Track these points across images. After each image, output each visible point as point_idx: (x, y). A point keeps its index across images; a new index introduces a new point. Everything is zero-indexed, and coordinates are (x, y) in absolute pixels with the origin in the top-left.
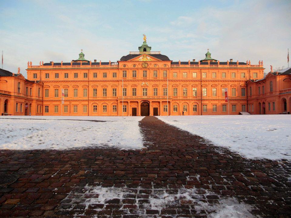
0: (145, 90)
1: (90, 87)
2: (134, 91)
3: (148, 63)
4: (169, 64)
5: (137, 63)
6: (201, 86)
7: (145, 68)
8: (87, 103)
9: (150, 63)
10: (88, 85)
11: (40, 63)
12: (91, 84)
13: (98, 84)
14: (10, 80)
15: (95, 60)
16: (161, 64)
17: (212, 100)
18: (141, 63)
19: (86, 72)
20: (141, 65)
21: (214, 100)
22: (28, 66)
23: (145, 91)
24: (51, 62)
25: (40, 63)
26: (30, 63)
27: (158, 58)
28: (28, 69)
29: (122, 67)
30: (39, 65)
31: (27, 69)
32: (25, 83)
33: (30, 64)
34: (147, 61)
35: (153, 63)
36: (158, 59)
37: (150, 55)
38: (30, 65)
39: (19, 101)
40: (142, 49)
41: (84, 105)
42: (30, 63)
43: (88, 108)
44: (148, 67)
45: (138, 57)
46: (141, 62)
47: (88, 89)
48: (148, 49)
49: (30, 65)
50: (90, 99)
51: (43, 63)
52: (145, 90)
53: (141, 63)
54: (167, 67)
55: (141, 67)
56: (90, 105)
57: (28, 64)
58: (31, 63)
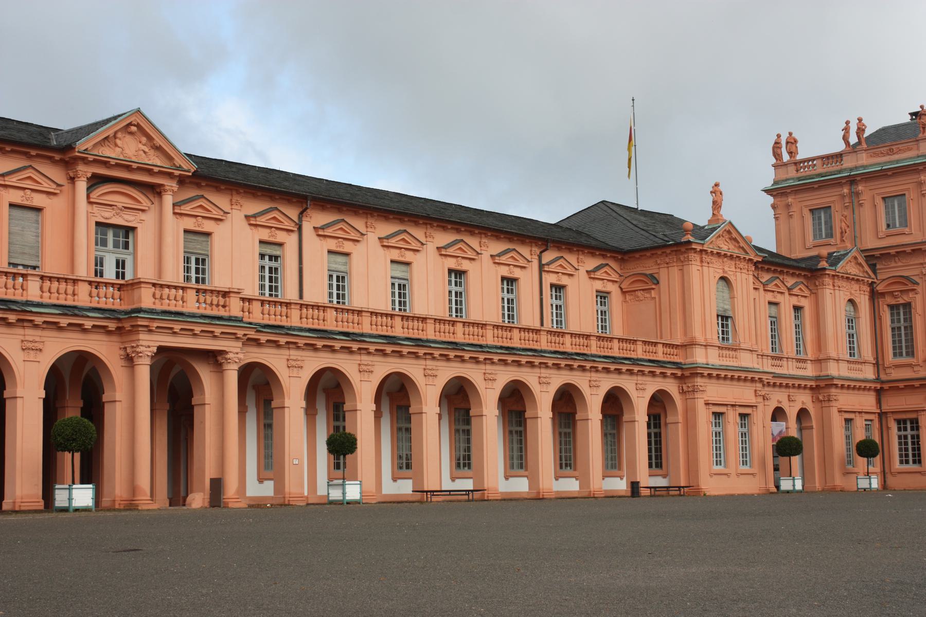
11: (846, 130)
14: (675, 271)
22: (779, 165)
24: (915, 115)
25: (846, 130)
26: (784, 149)
28: (775, 183)
30: (840, 147)
31: (769, 184)
32: (757, 278)
33: (784, 150)
38: (786, 157)
39: (730, 400)
42: (784, 149)
49: (786, 157)
51: (860, 130)
57: (777, 154)
58: (792, 142)
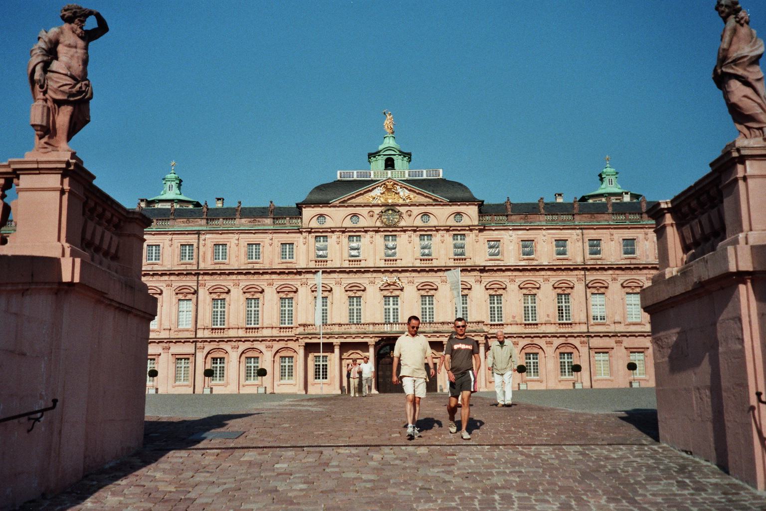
0: (391, 303)
1: (202, 292)
2: (355, 307)
3: (403, 210)
4: (471, 212)
5: (364, 211)
6: (587, 286)
7: (390, 227)
8: (189, 349)
9: (408, 208)
10: (194, 284)
12: (210, 282)
13: (297, 284)
15: (218, 199)
16: (442, 214)
17: (625, 335)
18: (377, 210)
19: (192, 239)
20: (376, 217)
21: (633, 335)
23: (391, 306)
27: (433, 192)
29: (314, 224)
34: (398, 205)
35: (416, 210)
36: (435, 196)
37: (407, 181)
40: (380, 162)
41: (179, 358)
43: (191, 366)
44: (402, 223)
45: (362, 190)
46: (378, 206)
47: (194, 300)
48: (399, 161)
50: (200, 334)
52: (391, 303)
53: (377, 210)
54: (466, 221)
55: (378, 224)
56: (200, 356)
